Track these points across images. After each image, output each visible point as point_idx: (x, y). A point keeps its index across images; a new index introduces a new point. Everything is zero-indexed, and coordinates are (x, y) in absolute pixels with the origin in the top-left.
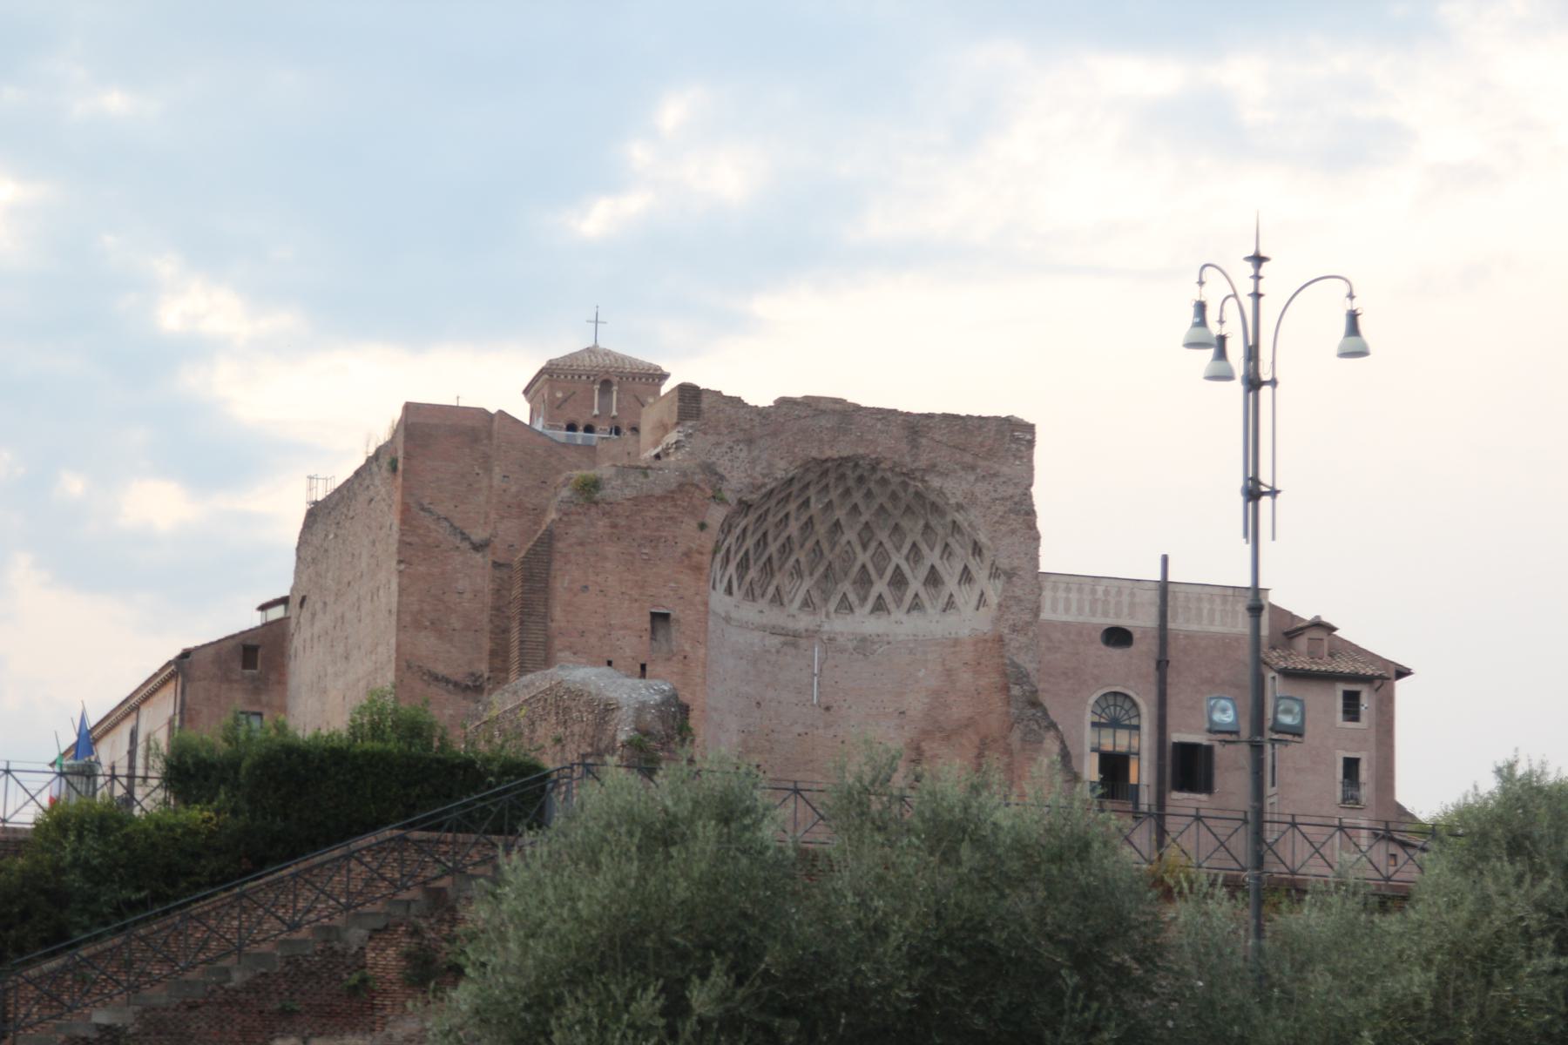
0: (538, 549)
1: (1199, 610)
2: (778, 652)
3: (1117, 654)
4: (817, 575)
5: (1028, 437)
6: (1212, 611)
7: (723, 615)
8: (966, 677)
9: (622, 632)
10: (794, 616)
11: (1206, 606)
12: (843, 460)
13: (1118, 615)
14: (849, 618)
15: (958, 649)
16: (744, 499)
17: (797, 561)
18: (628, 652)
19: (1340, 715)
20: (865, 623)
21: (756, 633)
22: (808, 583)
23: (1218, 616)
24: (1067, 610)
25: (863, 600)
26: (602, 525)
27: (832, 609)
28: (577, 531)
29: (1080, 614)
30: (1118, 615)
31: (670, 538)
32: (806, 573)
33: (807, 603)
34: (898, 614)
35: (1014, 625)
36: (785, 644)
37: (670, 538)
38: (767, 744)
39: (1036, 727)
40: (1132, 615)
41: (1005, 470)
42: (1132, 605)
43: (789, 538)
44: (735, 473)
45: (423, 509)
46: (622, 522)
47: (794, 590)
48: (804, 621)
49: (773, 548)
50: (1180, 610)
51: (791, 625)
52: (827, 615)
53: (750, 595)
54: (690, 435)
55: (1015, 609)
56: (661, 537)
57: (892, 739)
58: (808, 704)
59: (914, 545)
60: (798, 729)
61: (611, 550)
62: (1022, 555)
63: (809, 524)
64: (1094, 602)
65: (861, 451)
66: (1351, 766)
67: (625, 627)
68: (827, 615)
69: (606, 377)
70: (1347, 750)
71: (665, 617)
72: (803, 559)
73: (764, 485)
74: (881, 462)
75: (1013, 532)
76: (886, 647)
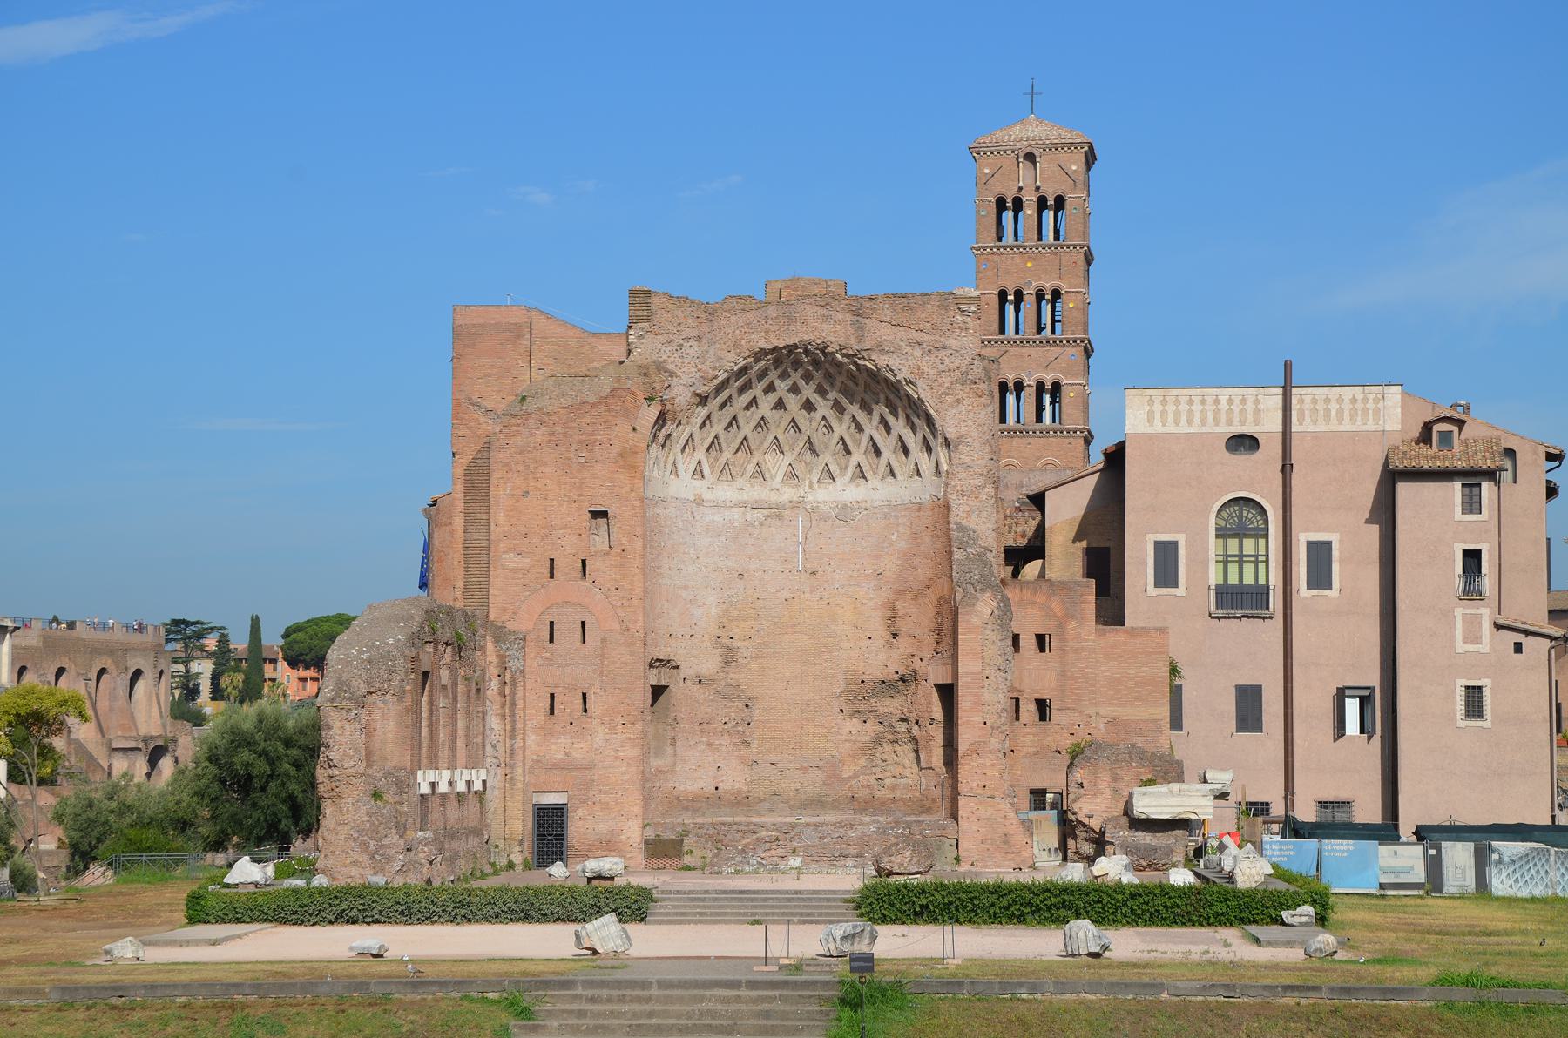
0: (477, 461)
1: (1328, 411)
2: (761, 525)
3: (1242, 460)
4: (797, 450)
5: (973, 309)
6: (1340, 411)
7: (692, 499)
8: (927, 540)
9: (561, 532)
10: (777, 490)
11: (1334, 407)
12: (791, 349)
13: (1243, 423)
14: (831, 487)
15: (921, 513)
16: (698, 391)
17: (776, 438)
18: (569, 550)
19: (1458, 509)
20: (846, 491)
21: (735, 510)
22: (789, 457)
23: (1347, 414)
24: (1190, 422)
25: (844, 469)
26: (540, 434)
27: (815, 480)
28: (519, 439)
29: (1203, 425)
30: (1243, 423)
31: (605, 441)
32: (786, 449)
33: (792, 475)
34: (874, 481)
35: (962, 490)
36: (767, 517)
37: (605, 441)
38: (752, 611)
39: (972, 590)
40: (1256, 422)
41: (952, 342)
42: (1257, 412)
43: (763, 418)
44: (685, 369)
45: (473, 405)
46: (560, 430)
47: (777, 465)
48: (788, 494)
49: (747, 430)
50: (1306, 412)
51: (774, 498)
52: (811, 486)
53: (726, 471)
54: (641, 337)
55: (963, 475)
56: (597, 439)
57: (872, 599)
58: (794, 571)
59: (882, 417)
60: (786, 594)
61: (549, 456)
62: (970, 423)
63: (780, 405)
64: (1217, 412)
65: (806, 338)
66: (1472, 558)
67: (565, 527)
68: (811, 486)
69: (1028, 150)
70: (1465, 543)
71: (604, 514)
72: (779, 437)
73: (716, 377)
74: (828, 346)
75: (959, 401)
76: (865, 512)
